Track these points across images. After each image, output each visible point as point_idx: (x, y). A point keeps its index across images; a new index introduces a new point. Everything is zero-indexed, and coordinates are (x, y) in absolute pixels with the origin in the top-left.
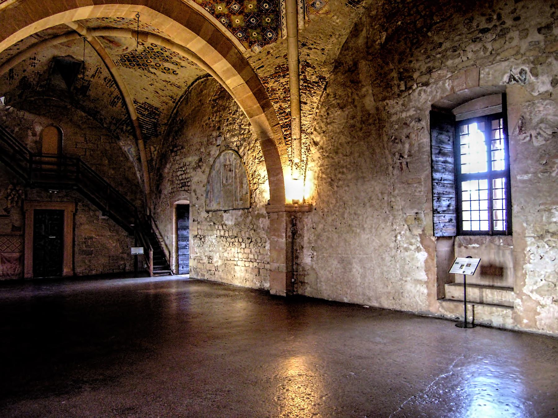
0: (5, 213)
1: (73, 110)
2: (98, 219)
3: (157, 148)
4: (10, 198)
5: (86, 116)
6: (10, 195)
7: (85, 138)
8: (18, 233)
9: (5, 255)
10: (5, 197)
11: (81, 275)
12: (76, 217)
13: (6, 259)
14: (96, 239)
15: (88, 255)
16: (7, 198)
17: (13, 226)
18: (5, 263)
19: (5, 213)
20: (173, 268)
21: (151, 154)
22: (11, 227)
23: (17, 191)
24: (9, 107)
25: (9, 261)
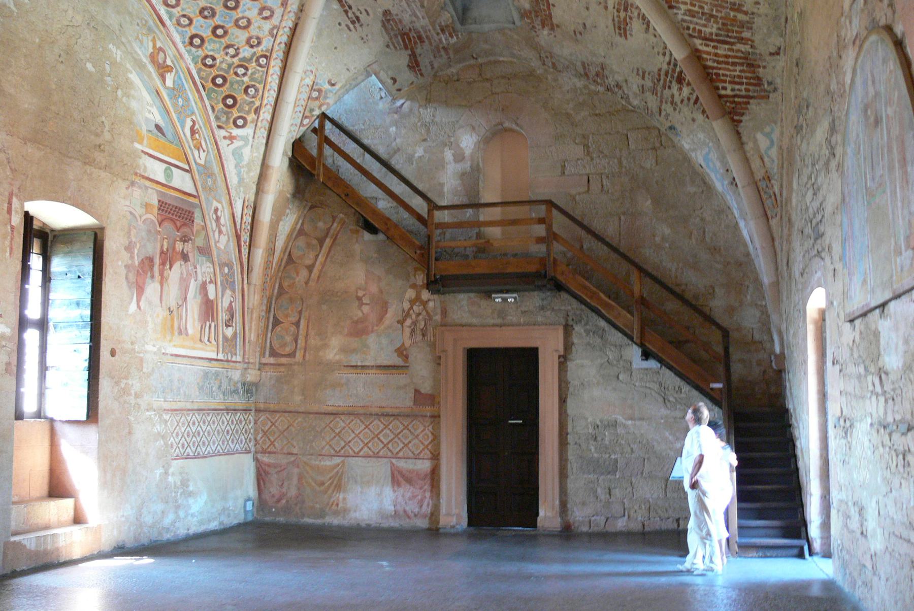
0: (399, 361)
1: (549, 77)
2: (629, 370)
3: (775, 136)
4: (408, 322)
5: (586, 87)
6: (408, 315)
7: (586, 146)
8: (428, 410)
9: (402, 464)
10: (398, 322)
11: (585, 529)
12: (570, 365)
13: (400, 472)
14: (625, 426)
15: (602, 474)
16: (401, 322)
17: (417, 391)
18: (399, 485)
19: (399, 361)
20: (814, 531)
21: (762, 159)
22: (412, 395)
23: (425, 304)
24: (401, 101)
25: (409, 481)
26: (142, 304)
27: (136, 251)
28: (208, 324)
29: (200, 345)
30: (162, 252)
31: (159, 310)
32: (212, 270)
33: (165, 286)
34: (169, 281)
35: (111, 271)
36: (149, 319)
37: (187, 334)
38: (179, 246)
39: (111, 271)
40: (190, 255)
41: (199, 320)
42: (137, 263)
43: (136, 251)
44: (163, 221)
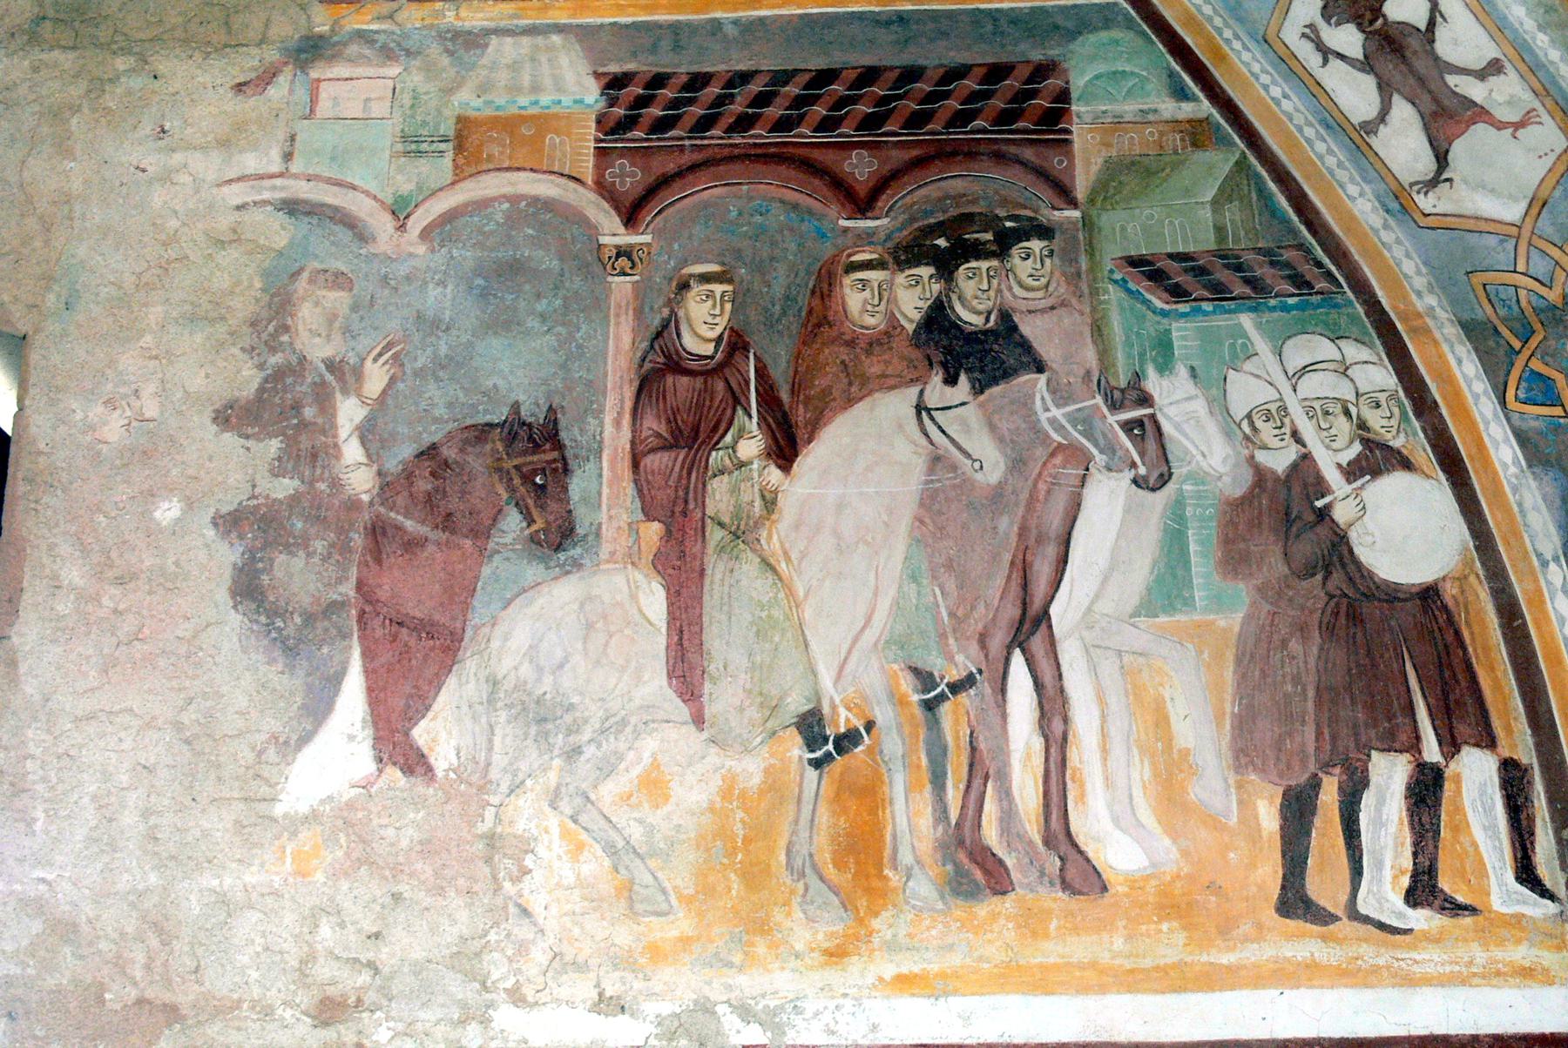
26: (441, 732)
27: (350, 413)
28: (1390, 776)
29: (1301, 944)
30: (662, 364)
31: (670, 741)
32: (1380, 377)
33: (733, 587)
34: (774, 539)
35: (73, 574)
36: (527, 814)
37: (1079, 875)
38: (893, 298)
39: (73, 574)
40: (1029, 328)
41: (1244, 755)
42: (360, 480)
43: (350, 413)
44: (651, 192)
